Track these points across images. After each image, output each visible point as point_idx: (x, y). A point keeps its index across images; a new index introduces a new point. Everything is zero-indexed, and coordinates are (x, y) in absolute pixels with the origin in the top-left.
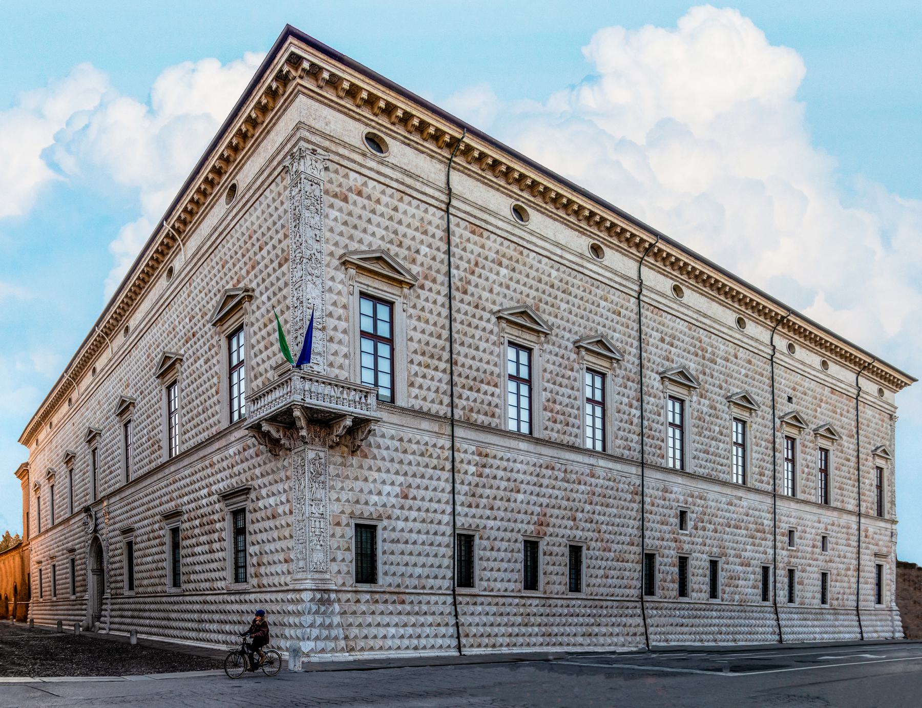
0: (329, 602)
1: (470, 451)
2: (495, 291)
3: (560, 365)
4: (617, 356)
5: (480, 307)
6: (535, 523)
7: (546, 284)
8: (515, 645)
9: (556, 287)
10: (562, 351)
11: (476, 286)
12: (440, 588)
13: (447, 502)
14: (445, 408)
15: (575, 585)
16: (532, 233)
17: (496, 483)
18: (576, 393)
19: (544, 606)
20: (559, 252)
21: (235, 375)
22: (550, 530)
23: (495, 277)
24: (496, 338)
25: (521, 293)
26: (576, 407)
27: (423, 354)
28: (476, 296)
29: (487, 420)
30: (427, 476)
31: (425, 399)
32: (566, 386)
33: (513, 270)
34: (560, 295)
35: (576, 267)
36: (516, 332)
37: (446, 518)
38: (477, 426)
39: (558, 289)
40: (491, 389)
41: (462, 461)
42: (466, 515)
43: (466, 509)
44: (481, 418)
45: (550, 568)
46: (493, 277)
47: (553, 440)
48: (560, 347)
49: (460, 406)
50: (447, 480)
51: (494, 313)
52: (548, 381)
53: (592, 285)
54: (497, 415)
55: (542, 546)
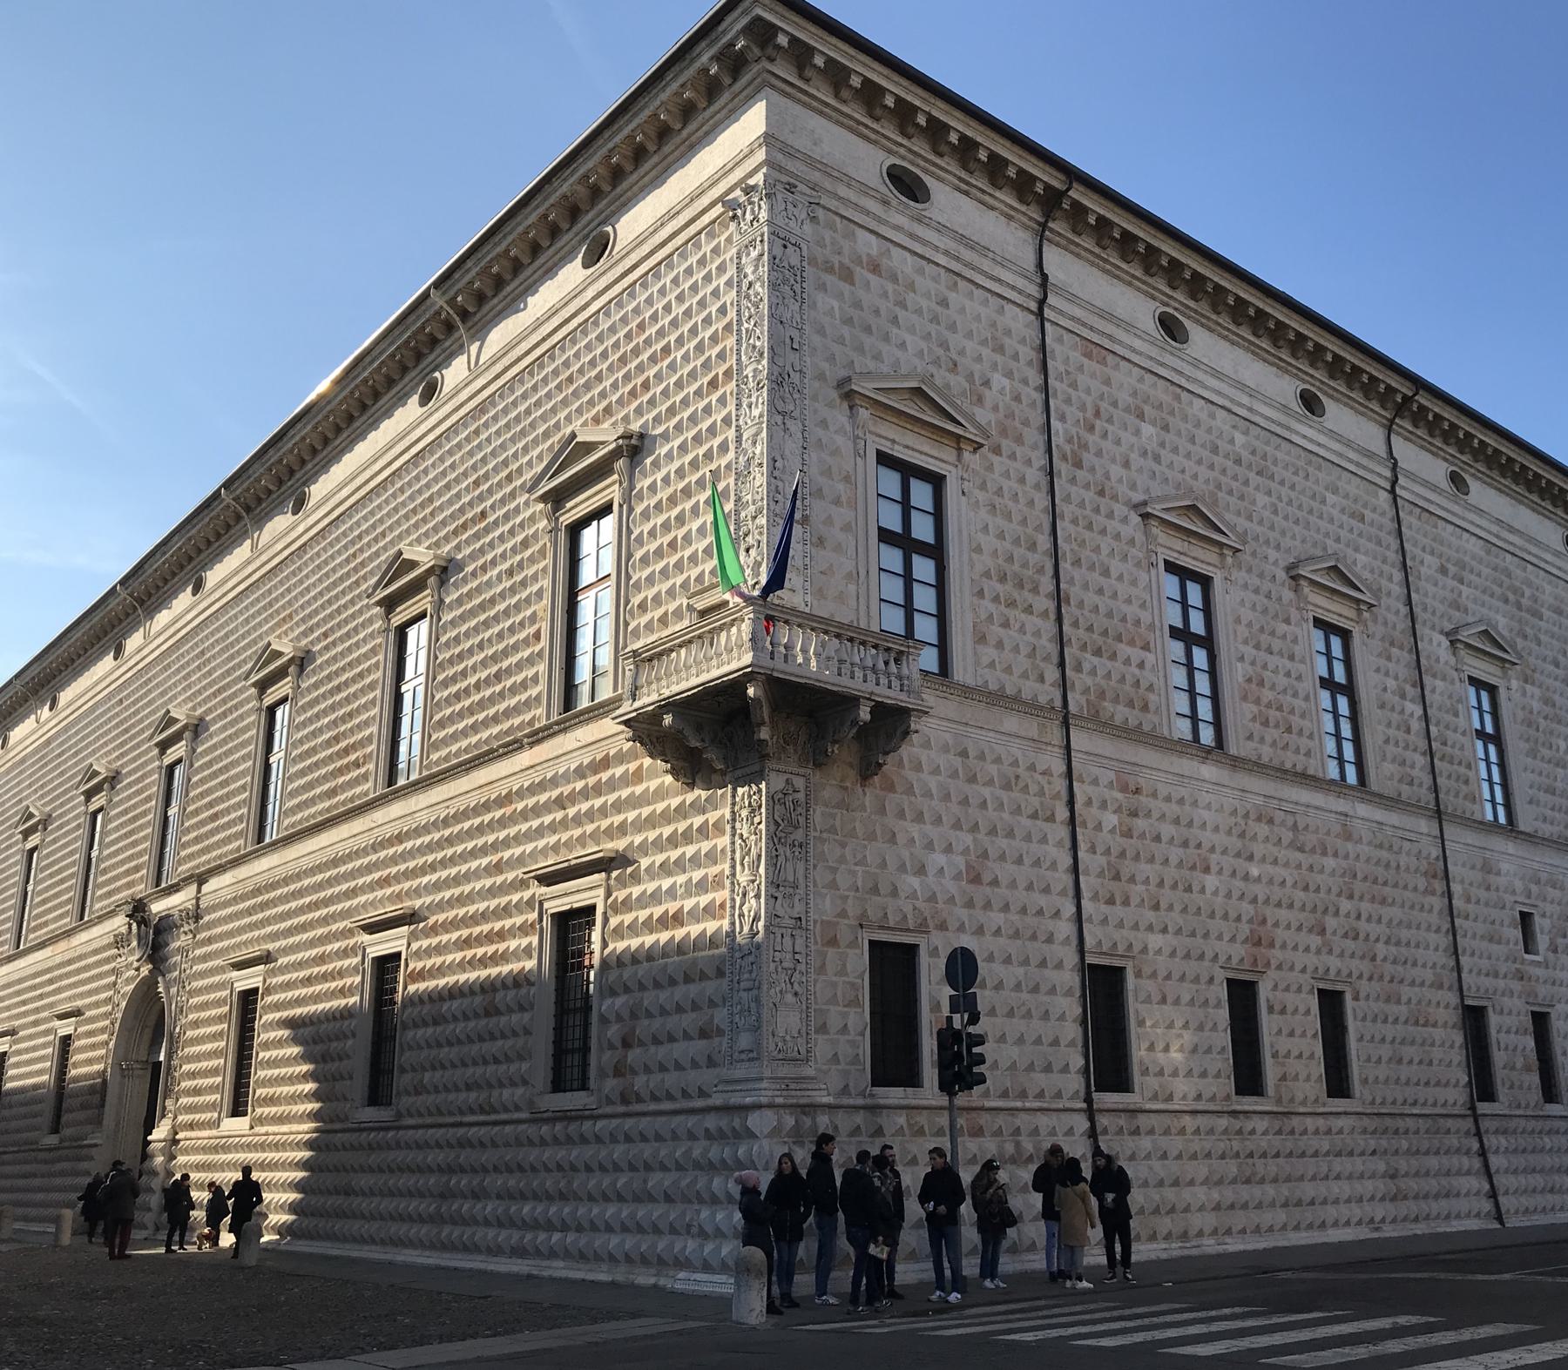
1: (1104, 781)
3: (1265, 611)
4: (1367, 597)
6: (1246, 941)
7: (1227, 456)
8: (1228, 1232)
10: (1266, 586)
11: (1099, 454)
12: (1059, 1095)
13: (1063, 893)
15: (1338, 1082)
17: (1159, 850)
18: (1302, 667)
19: (1279, 1132)
20: (1245, 400)
22: (1276, 955)
23: (1134, 439)
26: (1302, 694)
27: (1003, 579)
29: (1133, 717)
31: (1008, 670)
32: (1280, 653)
33: (1166, 428)
35: (1279, 430)
36: (1178, 545)
37: (1065, 929)
39: (1250, 467)
40: (1135, 654)
41: (1089, 802)
42: (1105, 921)
43: (1104, 908)
44: (1121, 713)
45: (1284, 1044)
46: (1127, 437)
47: (1265, 760)
48: (1261, 576)
50: (1060, 844)
51: (1135, 507)
52: (1246, 642)
53: (1309, 463)
54: (1152, 707)
55: (1264, 992)
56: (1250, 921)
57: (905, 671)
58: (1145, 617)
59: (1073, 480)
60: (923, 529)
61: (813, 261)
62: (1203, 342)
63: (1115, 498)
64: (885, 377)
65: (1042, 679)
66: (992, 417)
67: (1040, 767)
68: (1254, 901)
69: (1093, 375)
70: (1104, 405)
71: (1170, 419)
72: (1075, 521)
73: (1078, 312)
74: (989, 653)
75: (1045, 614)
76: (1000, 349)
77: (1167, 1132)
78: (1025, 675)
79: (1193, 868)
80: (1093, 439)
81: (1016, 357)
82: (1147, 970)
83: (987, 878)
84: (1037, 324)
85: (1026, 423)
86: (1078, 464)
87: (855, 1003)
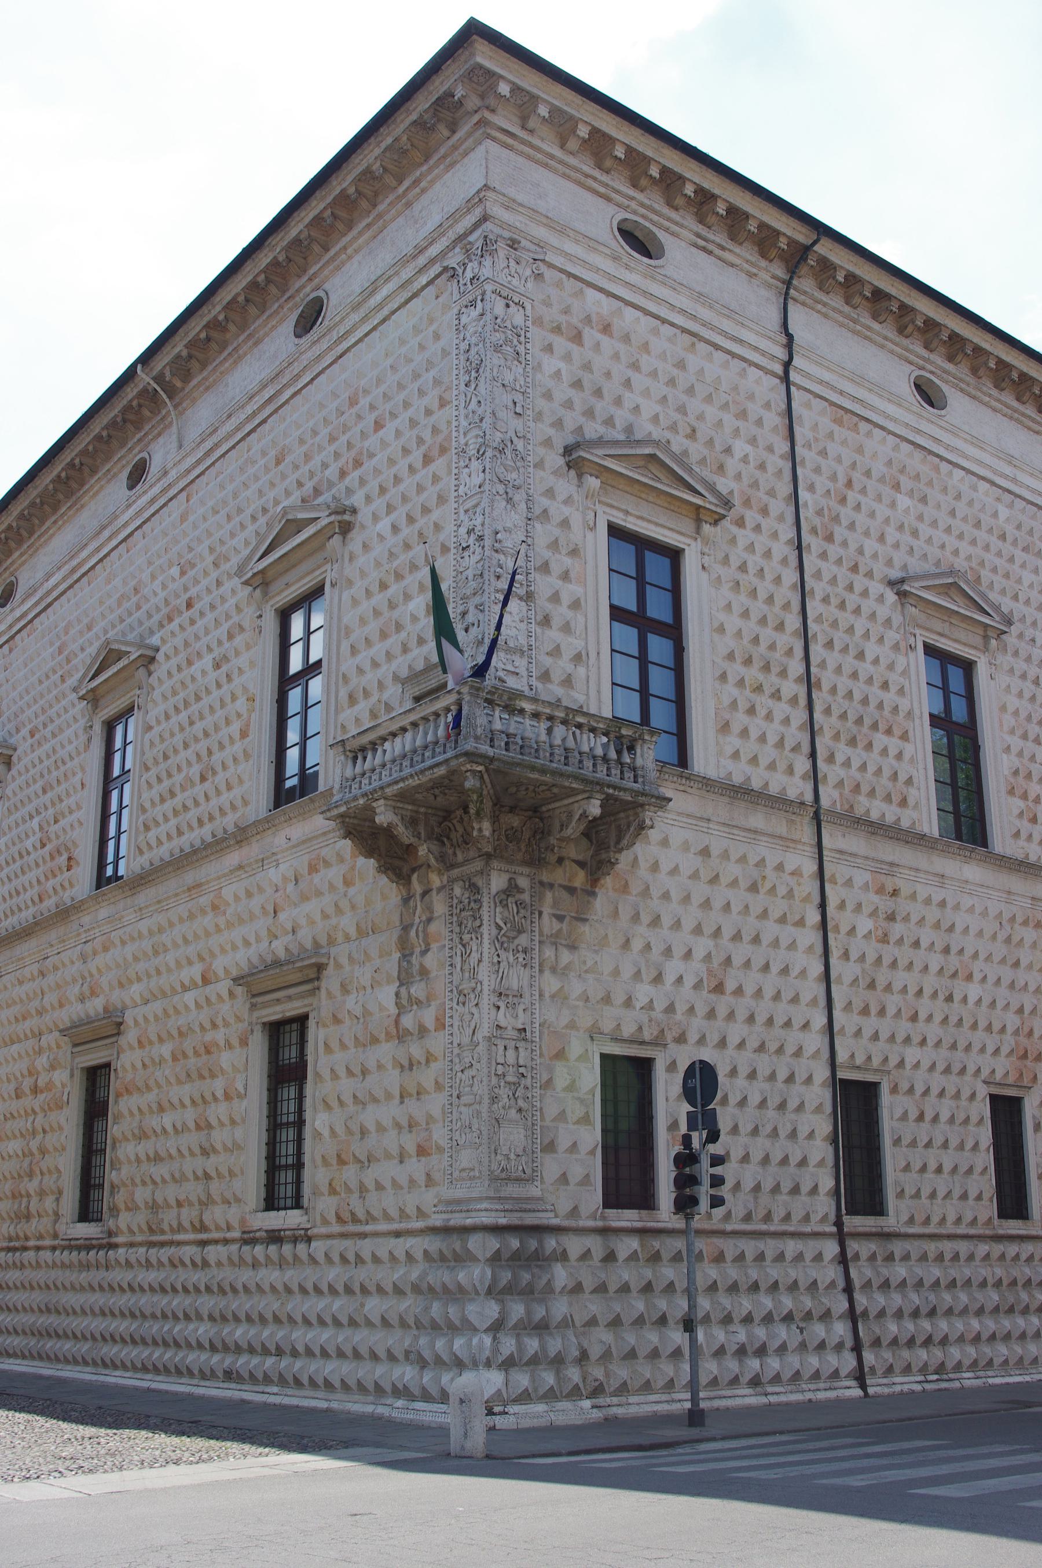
0: (538, 1259)
2: (890, 540)
5: (862, 569)
7: (990, 531)
9: (1009, 538)
14: (800, 783)
16: (954, 431)
17: (919, 957)
20: (1008, 470)
21: (295, 696)
24: (898, 636)
25: (943, 547)
28: (853, 546)
29: (892, 814)
30: (766, 939)
31: (754, 760)
33: (924, 500)
34: (1020, 556)
36: (938, 626)
37: (815, 1042)
38: (871, 824)
40: (893, 744)
41: (842, 906)
42: (858, 1033)
44: (876, 809)
46: (882, 511)
49: (832, 780)
51: (891, 584)
52: (1012, 732)
54: (911, 802)
55: (1030, 1111)
56: (1016, 1032)
57: (639, 762)
58: (904, 704)
59: (824, 555)
60: (658, 608)
61: (539, 322)
62: (960, 407)
63: (869, 574)
64: (616, 443)
65: (790, 770)
66: (733, 485)
67: (789, 867)
68: (1020, 1011)
69: (844, 443)
70: (857, 476)
71: (928, 491)
72: (826, 600)
73: (827, 376)
74: (733, 741)
75: (794, 701)
76: (743, 415)
77: (924, 1258)
78: (772, 766)
79: (954, 975)
80: (846, 513)
81: (759, 422)
82: (904, 1086)
83: (730, 986)
84: (783, 387)
85: (771, 493)
86: (829, 538)
87: (586, 1120)
